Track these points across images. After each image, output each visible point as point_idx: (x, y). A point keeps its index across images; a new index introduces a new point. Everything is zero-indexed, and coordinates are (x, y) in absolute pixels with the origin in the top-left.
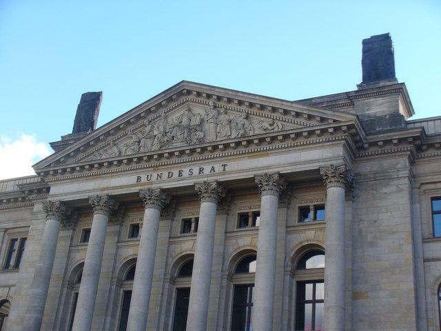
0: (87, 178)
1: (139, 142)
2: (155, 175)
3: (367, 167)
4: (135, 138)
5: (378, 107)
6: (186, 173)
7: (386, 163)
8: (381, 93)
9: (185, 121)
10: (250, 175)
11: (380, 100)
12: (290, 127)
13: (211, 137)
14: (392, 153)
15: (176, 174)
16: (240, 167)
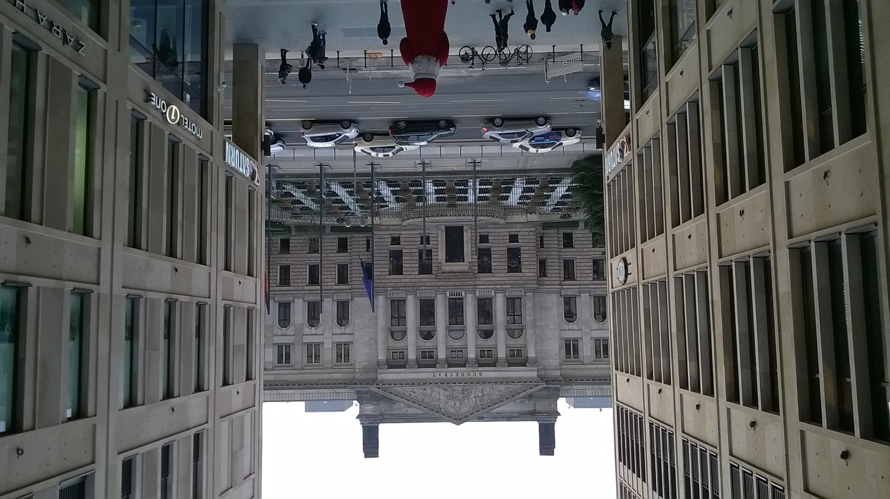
0: (512, 378)
1: (483, 395)
2: (472, 374)
3: (371, 376)
4: (486, 398)
5: (370, 409)
6: (454, 375)
7: (365, 377)
8: (367, 416)
9: (458, 404)
10: (420, 370)
11: (368, 413)
12: (399, 389)
13: (442, 392)
14: (361, 380)
15: (460, 374)
16: (425, 374)
